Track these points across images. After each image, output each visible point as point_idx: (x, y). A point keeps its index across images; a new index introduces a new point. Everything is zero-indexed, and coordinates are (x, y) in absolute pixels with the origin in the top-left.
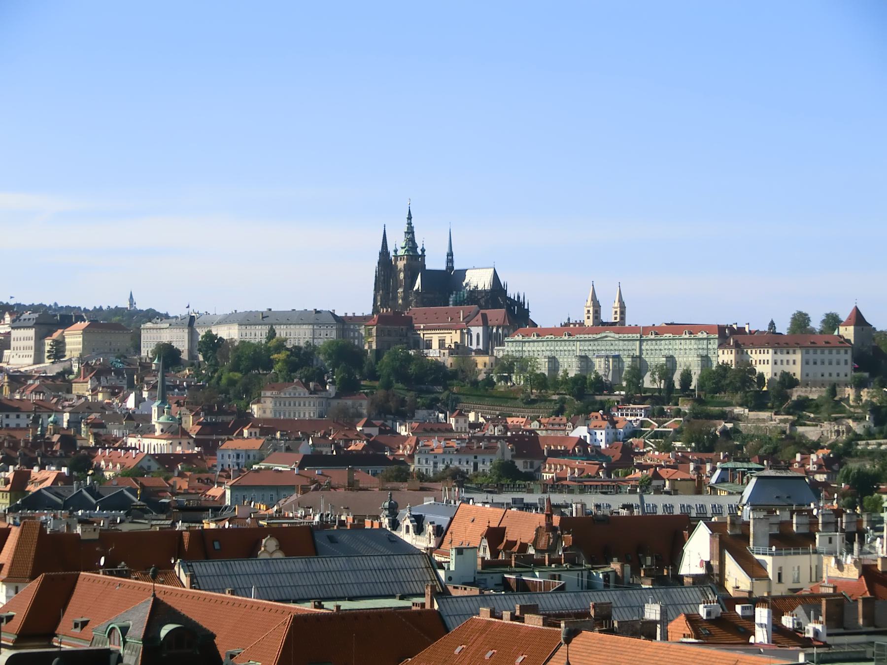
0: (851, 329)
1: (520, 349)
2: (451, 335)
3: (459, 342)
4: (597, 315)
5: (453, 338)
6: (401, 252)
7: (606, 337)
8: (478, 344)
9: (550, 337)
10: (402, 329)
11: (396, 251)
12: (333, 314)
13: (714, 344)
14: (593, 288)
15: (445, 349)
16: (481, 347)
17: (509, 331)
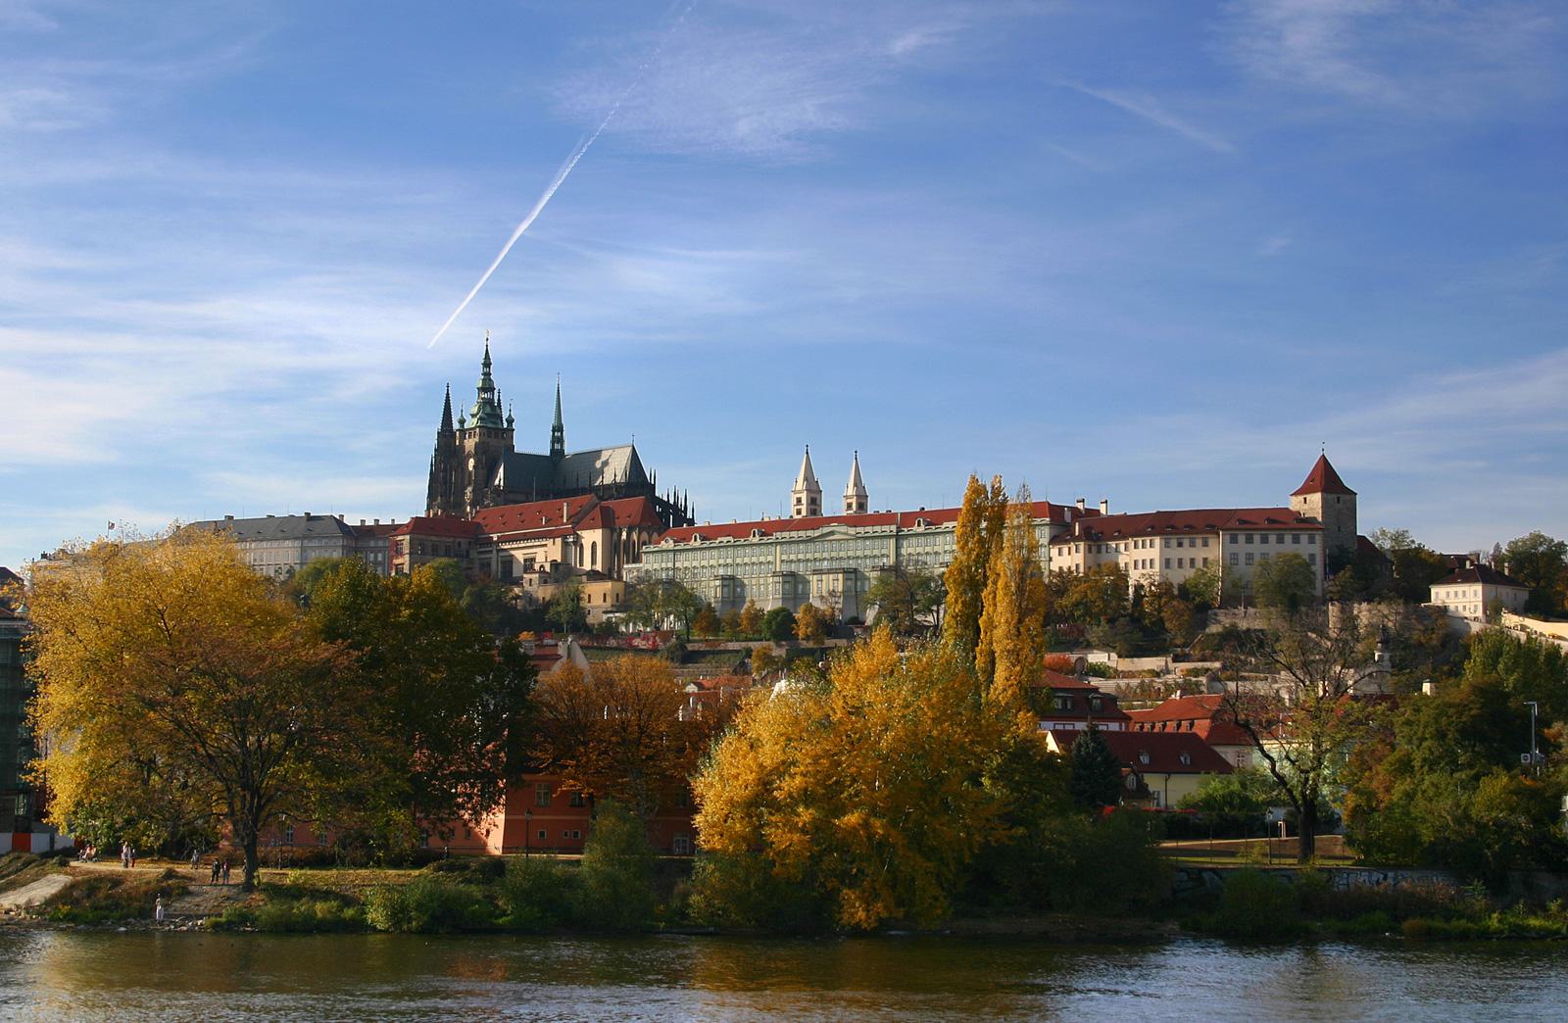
0: (1316, 498)
1: (670, 565)
2: (545, 549)
3: (559, 561)
4: (813, 507)
5: (547, 553)
6: (471, 423)
7: (832, 533)
8: (594, 562)
9: (725, 539)
10: (459, 544)
11: (462, 422)
12: (340, 522)
13: (1043, 535)
14: (808, 457)
15: (535, 572)
16: (599, 567)
17: (650, 536)
